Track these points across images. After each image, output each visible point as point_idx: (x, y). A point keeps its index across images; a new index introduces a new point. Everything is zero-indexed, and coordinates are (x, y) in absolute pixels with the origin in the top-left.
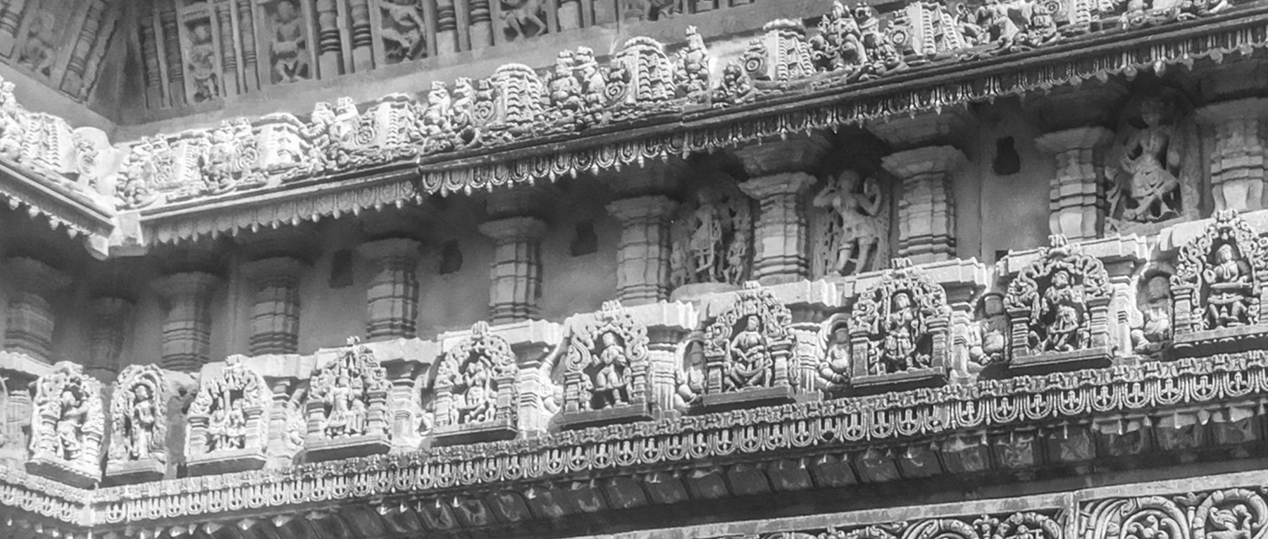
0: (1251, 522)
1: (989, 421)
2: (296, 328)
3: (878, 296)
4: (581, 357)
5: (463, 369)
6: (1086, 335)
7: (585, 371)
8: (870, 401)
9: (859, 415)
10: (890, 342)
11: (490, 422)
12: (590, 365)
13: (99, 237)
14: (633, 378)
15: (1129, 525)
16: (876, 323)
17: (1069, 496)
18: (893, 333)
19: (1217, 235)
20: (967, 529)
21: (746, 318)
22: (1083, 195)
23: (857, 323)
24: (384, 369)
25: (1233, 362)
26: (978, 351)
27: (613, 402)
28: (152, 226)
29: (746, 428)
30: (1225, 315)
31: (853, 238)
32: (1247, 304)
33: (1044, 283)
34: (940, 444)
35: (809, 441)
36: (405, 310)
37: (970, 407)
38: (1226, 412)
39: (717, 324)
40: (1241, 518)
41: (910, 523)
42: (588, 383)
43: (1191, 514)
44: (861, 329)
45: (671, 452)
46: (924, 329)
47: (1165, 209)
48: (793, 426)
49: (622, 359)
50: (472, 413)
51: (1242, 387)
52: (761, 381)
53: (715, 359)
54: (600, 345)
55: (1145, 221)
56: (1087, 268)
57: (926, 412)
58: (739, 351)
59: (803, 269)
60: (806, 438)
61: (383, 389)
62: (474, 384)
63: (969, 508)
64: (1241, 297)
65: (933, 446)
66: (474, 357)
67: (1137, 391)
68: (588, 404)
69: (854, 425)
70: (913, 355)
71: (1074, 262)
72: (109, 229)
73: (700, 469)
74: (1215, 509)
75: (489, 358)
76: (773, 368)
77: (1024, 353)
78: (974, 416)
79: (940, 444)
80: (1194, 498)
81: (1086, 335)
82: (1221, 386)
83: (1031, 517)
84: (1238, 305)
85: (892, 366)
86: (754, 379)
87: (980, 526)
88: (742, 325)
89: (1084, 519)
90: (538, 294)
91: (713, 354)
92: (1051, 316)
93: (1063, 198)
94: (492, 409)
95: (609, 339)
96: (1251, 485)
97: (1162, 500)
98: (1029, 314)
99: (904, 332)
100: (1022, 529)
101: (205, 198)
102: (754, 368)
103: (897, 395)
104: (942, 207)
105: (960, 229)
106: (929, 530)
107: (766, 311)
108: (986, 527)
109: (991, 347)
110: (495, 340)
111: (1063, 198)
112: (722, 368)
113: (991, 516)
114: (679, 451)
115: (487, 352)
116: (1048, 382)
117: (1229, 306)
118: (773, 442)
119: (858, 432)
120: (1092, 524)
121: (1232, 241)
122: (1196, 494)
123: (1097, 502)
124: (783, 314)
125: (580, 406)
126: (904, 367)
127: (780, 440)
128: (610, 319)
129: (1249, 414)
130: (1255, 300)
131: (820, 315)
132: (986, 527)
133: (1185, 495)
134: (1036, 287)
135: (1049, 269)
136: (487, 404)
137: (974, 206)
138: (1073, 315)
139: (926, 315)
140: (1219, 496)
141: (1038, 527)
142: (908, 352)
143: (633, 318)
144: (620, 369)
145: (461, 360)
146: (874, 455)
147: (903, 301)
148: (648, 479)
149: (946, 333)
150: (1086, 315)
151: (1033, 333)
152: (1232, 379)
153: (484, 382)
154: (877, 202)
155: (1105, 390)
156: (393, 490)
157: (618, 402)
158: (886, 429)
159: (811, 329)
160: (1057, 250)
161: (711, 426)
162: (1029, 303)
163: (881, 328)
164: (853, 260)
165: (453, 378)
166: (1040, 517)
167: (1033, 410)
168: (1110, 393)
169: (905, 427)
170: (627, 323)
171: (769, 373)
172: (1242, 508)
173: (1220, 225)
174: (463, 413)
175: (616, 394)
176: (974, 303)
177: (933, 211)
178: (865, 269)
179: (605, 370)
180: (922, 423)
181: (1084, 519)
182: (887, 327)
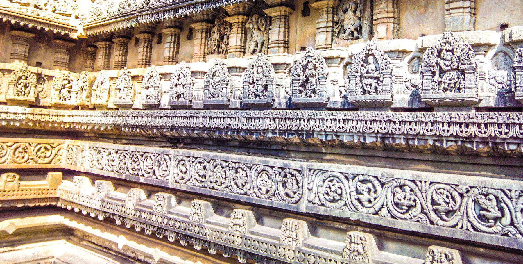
2: (126, 59)
8: (242, 113)
13: (73, 34)
15: (327, 183)
16: (251, 78)
17: (305, 164)
19: (367, 52)
22: (327, 27)
28: (86, 30)
31: (255, 40)
33: (305, 67)
36: (146, 56)
41: (254, 165)
43: (351, 182)
44: (246, 80)
47: (356, 34)
55: (348, 39)
59: (242, 50)
70: (262, 92)
71: (315, 59)
72: (76, 31)
73: (197, 130)
74: (359, 183)
80: (351, 176)
82: (362, 126)
83: (291, 171)
89: (310, 176)
90: (177, 53)
93: (320, 28)
96: (374, 175)
97: (339, 175)
98: (299, 80)
101: (95, 22)
104: (282, 29)
105: (290, 37)
106: (259, 169)
108: (277, 172)
111: (320, 28)
113: (279, 168)
122: (352, 174)
123: (315, 170)
131: (241, 70)
133: (348, 174)
134: (302, 69)
135: (306, 62)
137: (295, 28)
140: (361, 178)
142: (261, 91)
149: (272, 85)
150: (318, 82)
151: (301, 88)
154: (264, 25)
162: (299, 76)
164: (256, 48)
166: (295, 172)
176: (288, 70)
177: (279, 31)
178: (260, 51)
181: (310, 176)
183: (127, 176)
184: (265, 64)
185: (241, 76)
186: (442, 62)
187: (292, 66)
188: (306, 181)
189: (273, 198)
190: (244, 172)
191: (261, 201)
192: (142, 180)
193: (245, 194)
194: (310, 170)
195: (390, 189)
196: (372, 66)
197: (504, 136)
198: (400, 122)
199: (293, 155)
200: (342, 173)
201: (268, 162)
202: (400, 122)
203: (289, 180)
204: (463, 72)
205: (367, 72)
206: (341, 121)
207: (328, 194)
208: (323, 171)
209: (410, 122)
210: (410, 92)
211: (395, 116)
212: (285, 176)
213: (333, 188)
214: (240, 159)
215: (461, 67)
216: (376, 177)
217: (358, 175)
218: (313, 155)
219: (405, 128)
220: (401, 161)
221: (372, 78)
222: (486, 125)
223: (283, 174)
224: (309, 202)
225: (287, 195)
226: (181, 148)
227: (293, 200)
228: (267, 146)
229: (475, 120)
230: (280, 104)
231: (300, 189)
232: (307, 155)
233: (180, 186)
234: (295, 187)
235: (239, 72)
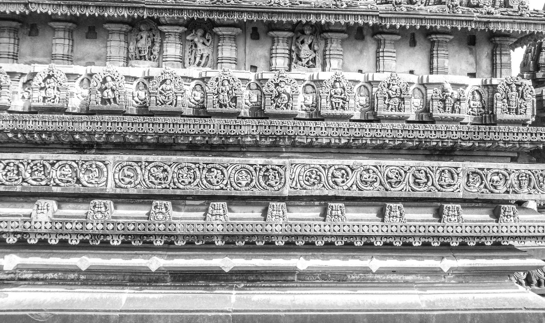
0: (346, 176)
1: (261, 133)
3: (217, 79)
4: (95, 83)
5: (44, 81)
6: (291, 105)
7: (99, 90)
9: (214, 125)
10: (221, 97)
11: (56, 104)
12: (101, 88)
14: (119, 96)
17: (287, 161)
18: (222, 94)
20: (251, 169)
21: (165, 80)
23: (209, 89)
24: (8, 76)
25: (345, 125)
26: (248, 101)
27: (110, 103)
29: (170, 124)
30: (337, 106)
32: (344, 103)
34: (242, 138)
35: (194, 132)
37: (255, 127)
38: (340, 140)
39: (154, 81)
40: (343, 174)
42: (100, 95)
43: (327, 171)
45: (139, 129)
46: (234, 95)
48: (188, 126)
49: (114, 87)
50: (49, 99)
51: (347, 134)
52: (171, 104)
53: (153, 93)
54: (105, 81)
56: (292, 82)
57: (239, 127)
58: (162, 91)
60: (193, 131)
61: (8, 84)
62: (49, 87)
63: (252, 161)
64: (342, 101)
65: (239, 138)
66: (49, 77)
67: (313, 130)
68: (100, 103)
69: (212, 128)
74: (335, 171)
75: (56, 78)
76: (176, 100)
77: (269, 108)
78: (256, 131)
79: (242, 138)
80: (328, 167)
81: (291, 105)
84: (341, 104)
85: (221, 106)
86: (169, 103)
87: (256, 168)
88: (164, 81)
91: (153, 91)
92: (279, 96)
94: (57, 99)
95: (109, 79)
97: (318, 166)
99: (226, 94)
100: (271, 170)
102: (168, 99)
103: (229, 120)
107: (174, 79)
108: (258, 169)
109: (253, 101)
110: (59, 72)
112: (156, 97)
113: (260, 165)
114: (142, 129)
115: (55, 76)
116: (283, 123)
117: (339, 103)
118: (180, 130)
119: (213, 131)
120: (294, 171)
121: (339, 82)
124: (180, 81)
125: (97, 103)
126: (226, 106)
127: (183, 130)
128: (109, 71)
129: (347, 141)
130: (347, 103)
132: (258, 169)
135: (279, 81)
136: (55, 96)
138: (287, 98)
139: (235, 90)
140: (337, 167)
141: (276, 170)
143: (119, 72)
144: (113, 91)
145: (44, 78)
146: (218, 139)
147: (226, 83)
148: (128, 136)
152: (344, 130)
153: (54, 87)
155: (302, 128)
156: (16, 129)
157: (113, 103)
158: (224, 131)
159: (188, 85)
160: (282, 75)
161: (156, 122)
163: (218, 92)
165: (40, 84)
166: (277, 167)
167: (277, 132)
168: (304, 129)
169: (231, 132)
170: (116, 74)
171: (175, 102)
172: (343, 171)
173: (337, 76)
174: (44, 98)
175: (112, 100)
179: (107, 90)
180: (237, 131)
182: (220, 92)
183: (24, 187)
184: (233, 79)
185: (189, 85)
186: (390, 92)
187: (252, 81)
188: (288, 174)
189: (254, 189)
190: (219, 171)
191: (241, 193)
192: (56, 190)
193: (222, 189)
194: (292, 164)
195: (359, 173)
196: (339, 90)
197: (433, 138)
198: (370, 129)
199: (249, 155)
200: (320, 165)
201: (248, 161)
202: (370, 129)
203: (271, 174)
204: (403, 99)
205: (335, 94)
206: (313, 128)
207: (308, 181)
208: (304, 165)
209: (377, 130)
210: (359, 109)
211: (367, 126)
212: (267, 170)
213: (313, 176)
214: (215, 160)
215: (402, 96)
216: (349, 166)
217: (333, 165)
218: (269, 154)
219: (373, 133)
220: (346, 155)
221: (339, 98)
222: (424, 131)
223: (264, 169)
224: (291, 188)
225: (269, 185)
226: (94, 154)
227: (276, 188)
228: (223, 148)
229: (418, 129)
230: (245, 113)
231: (283, 180)
232: (264, 154)
233: (128, 191)
234: (277, 178)
235: (189, 82)
